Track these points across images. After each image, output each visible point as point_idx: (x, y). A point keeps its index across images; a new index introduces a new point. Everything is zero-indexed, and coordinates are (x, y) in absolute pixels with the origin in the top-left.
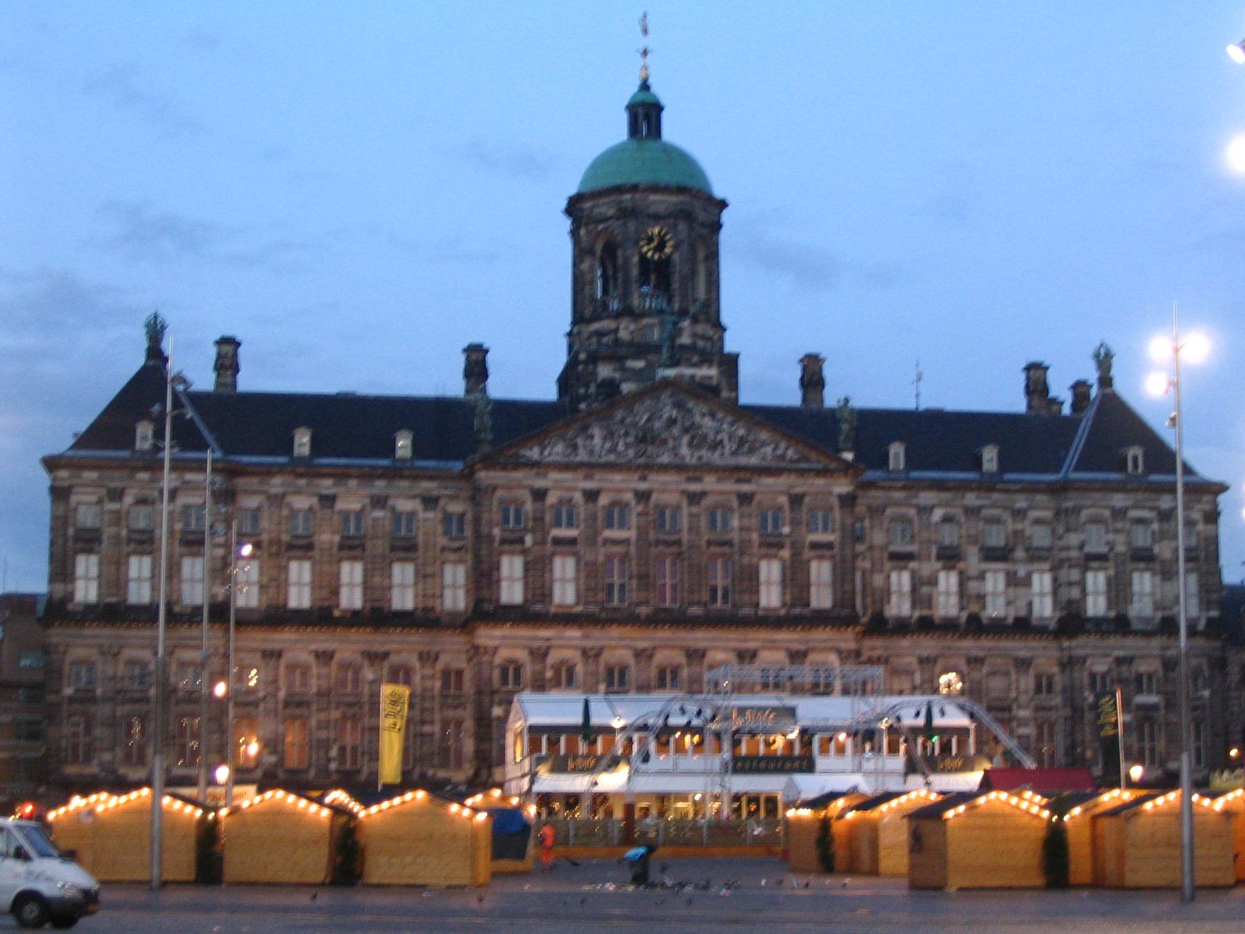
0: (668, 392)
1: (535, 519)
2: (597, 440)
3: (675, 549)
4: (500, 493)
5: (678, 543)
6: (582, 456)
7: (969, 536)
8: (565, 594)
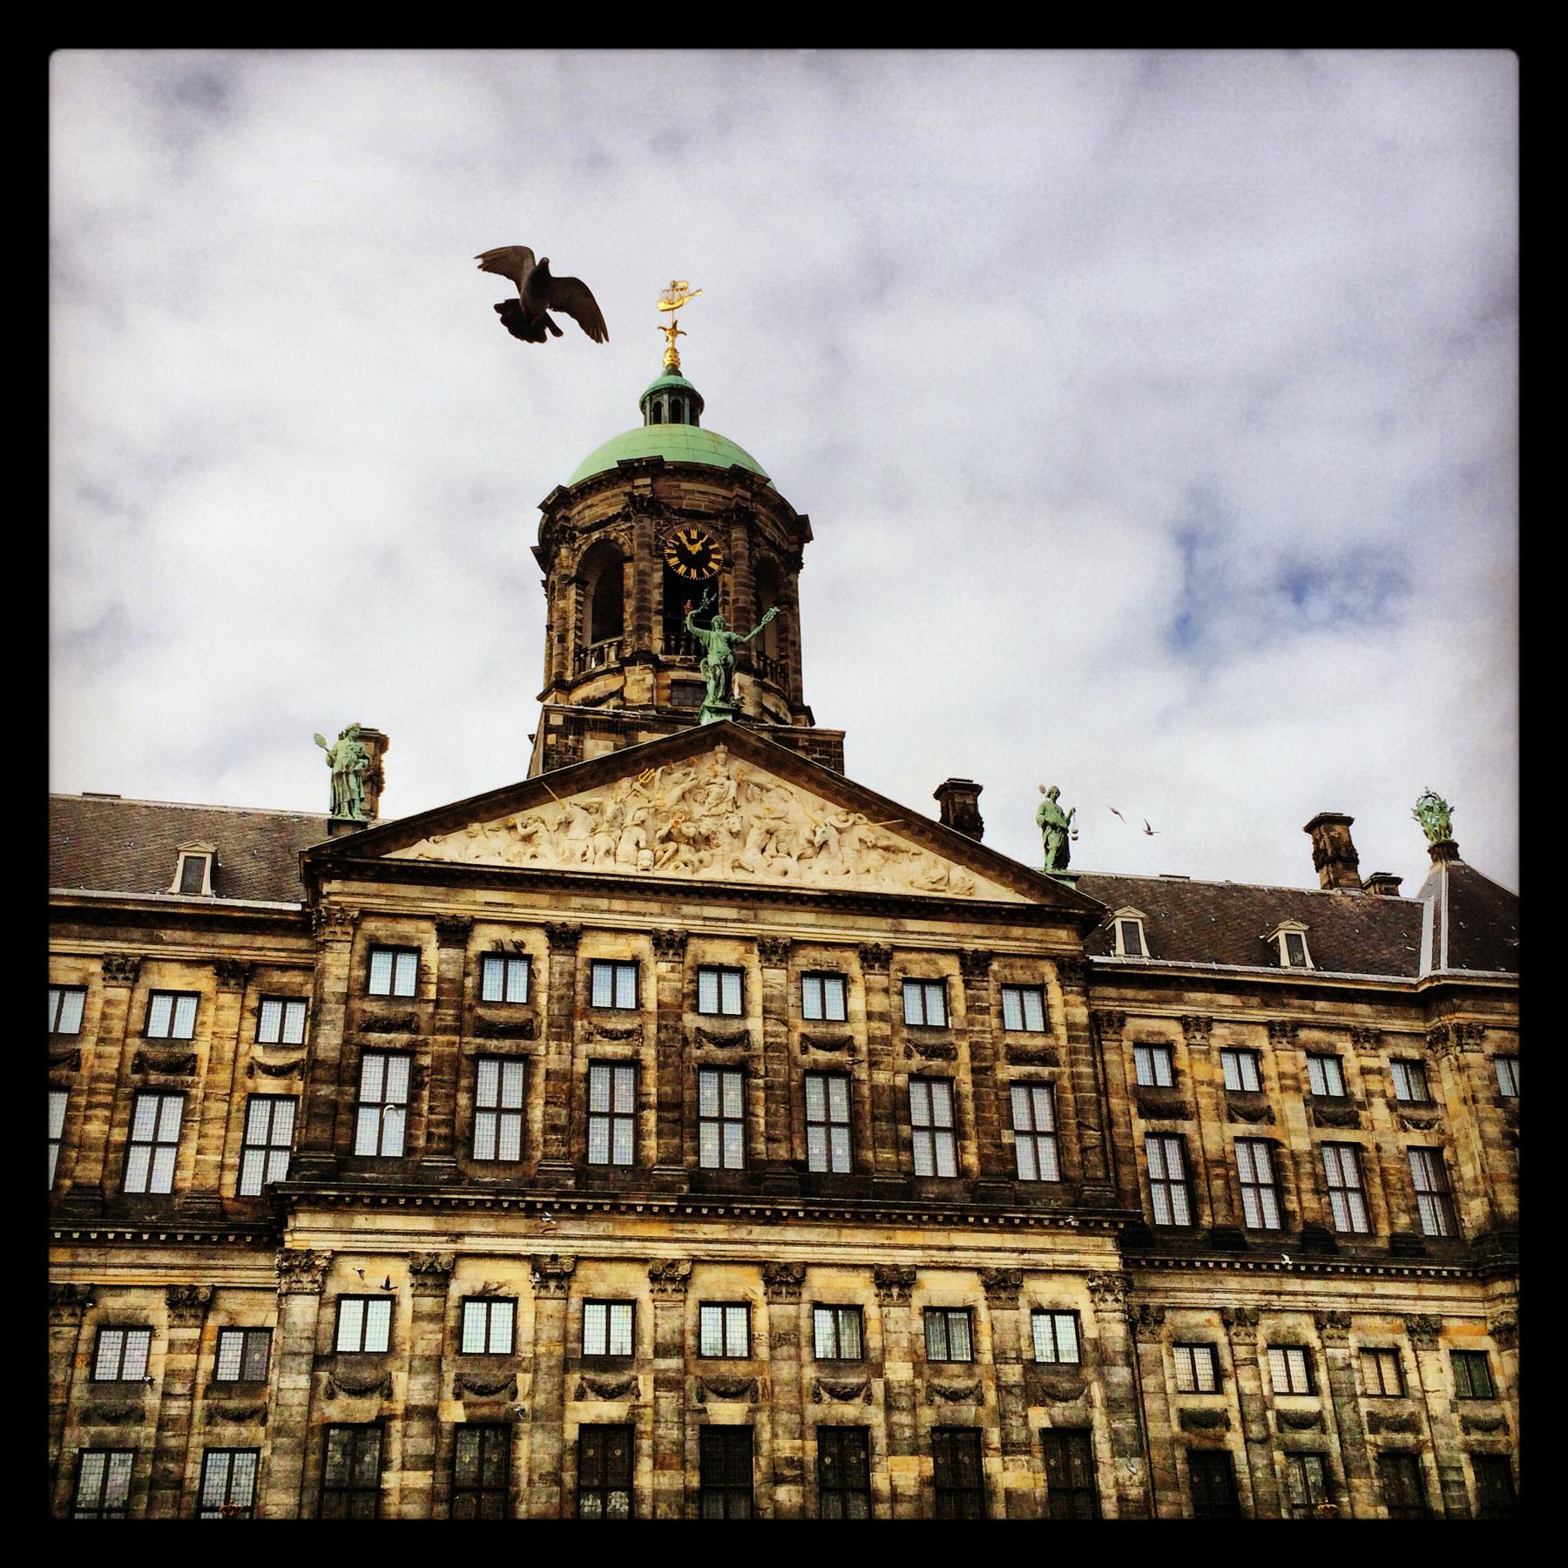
0: (721, 748)
1: (441, 980)
2: (579, 830)
3: (738, 1052)
4: (371, 926)
5: (743, 1038)
6: (549, 860)
7: (1281, 1076)
8: (497, 1141)
